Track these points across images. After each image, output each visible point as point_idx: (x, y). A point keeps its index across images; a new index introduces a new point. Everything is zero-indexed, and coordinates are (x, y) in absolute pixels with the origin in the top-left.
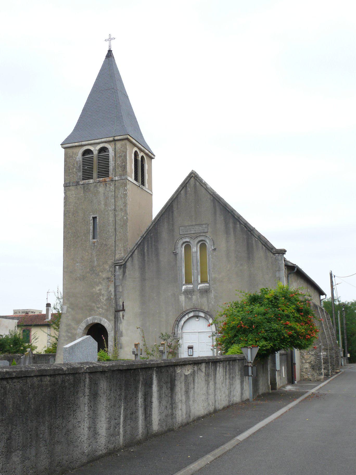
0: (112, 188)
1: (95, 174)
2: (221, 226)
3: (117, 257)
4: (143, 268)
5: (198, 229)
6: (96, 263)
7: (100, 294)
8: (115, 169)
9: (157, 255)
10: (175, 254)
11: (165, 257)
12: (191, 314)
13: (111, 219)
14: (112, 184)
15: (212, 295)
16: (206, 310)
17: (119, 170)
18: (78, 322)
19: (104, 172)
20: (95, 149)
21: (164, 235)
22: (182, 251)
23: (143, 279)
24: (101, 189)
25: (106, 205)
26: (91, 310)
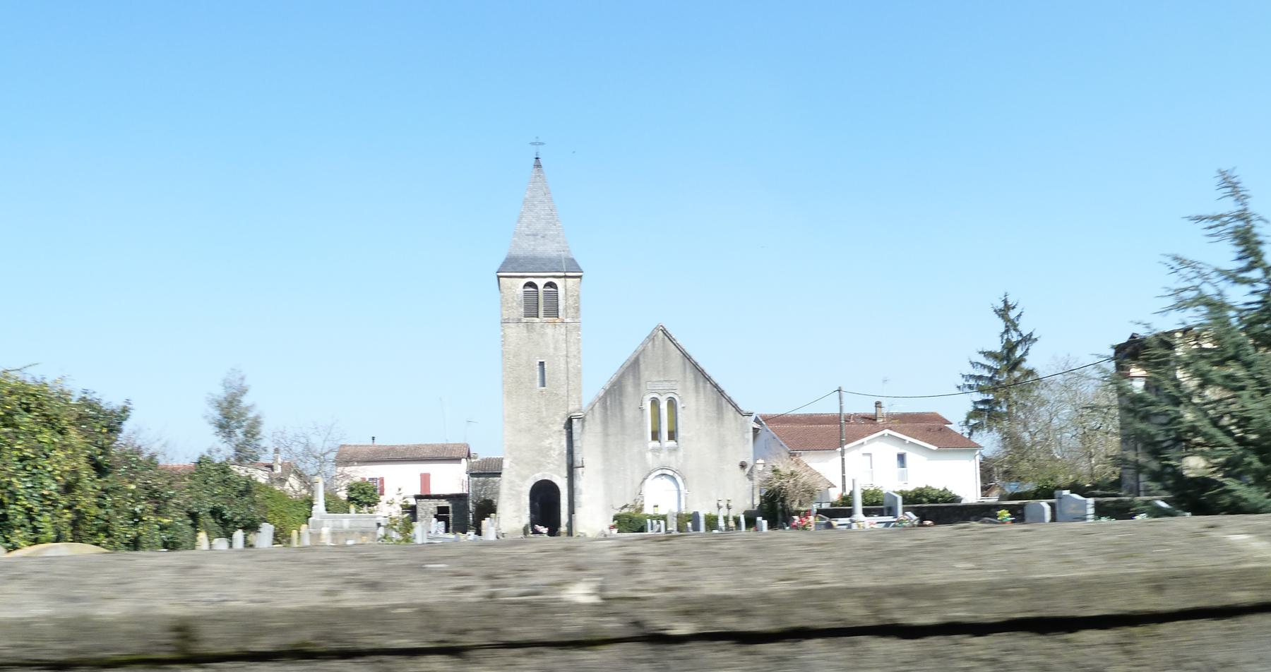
0: (563, 330)
1: (541, 313)
2: (690, 383)
3: (571, 408)
4: (605, 422)
5: (667, 386)
6: (544, 414)
7: (551, 448)
8: (565, 309)
9: (622, 409)
10: (642, 410)
11: (630, 412)
12: (660, 472)
13: (563, 366)
14: (563, 326)
15: (681, 454)
16: (674, 468)
17: (571, 311)
18: (525, 478)
19: (553, 311)
20: (541, 283)
21: (629, 388)
22: (647, 406)
23: (606, 435)
24: (549, 330)
25: (556, 349)
26: (540, 466)
